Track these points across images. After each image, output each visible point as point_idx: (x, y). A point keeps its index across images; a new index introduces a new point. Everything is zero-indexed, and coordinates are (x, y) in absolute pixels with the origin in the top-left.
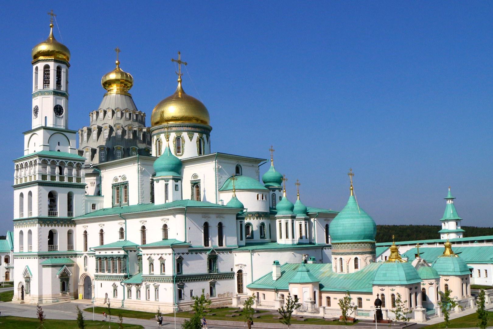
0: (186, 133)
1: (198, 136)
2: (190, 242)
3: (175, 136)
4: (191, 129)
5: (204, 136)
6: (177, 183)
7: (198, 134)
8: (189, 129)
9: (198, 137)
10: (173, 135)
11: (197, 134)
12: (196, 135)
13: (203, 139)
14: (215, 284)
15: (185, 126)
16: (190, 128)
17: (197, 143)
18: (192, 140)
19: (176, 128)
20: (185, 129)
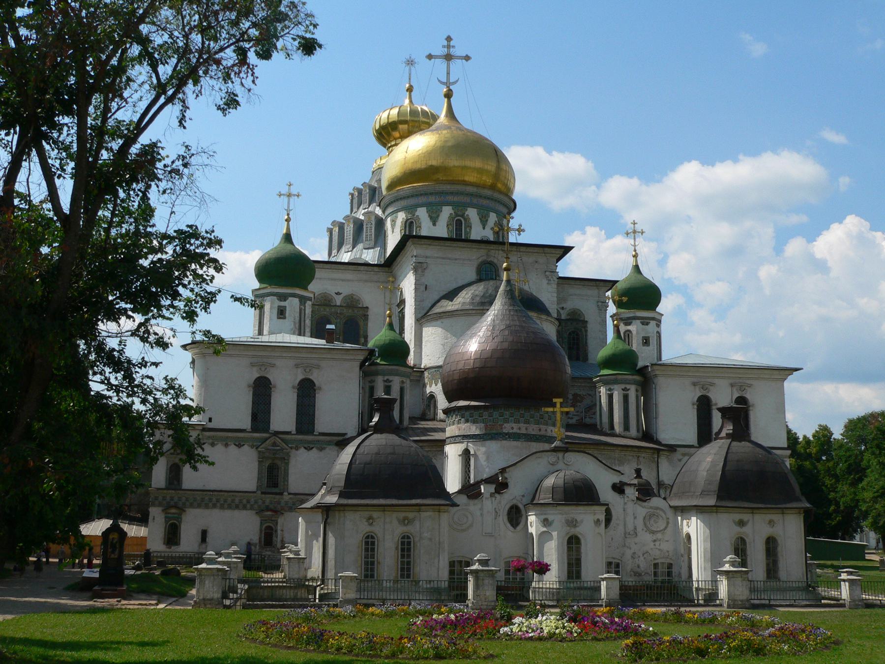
0: (425, 208)
1: (452, 212)
2: (210, 420)
3: (403, 218)
4: (434, 200)
5: (472, 214)
6: (283, 304)
7: (453, 209)
8: (432, 199)
9: (451, 214)
10: (401, 216)
11: (451, 207)
12: (447, 212)
13: (467, 220)
14: (277, 520)
15: (421, 195)
16: (433, 198)
17: (448, 228)
18: (437, 223)
19: (406, 201)
20: (423, 199)
